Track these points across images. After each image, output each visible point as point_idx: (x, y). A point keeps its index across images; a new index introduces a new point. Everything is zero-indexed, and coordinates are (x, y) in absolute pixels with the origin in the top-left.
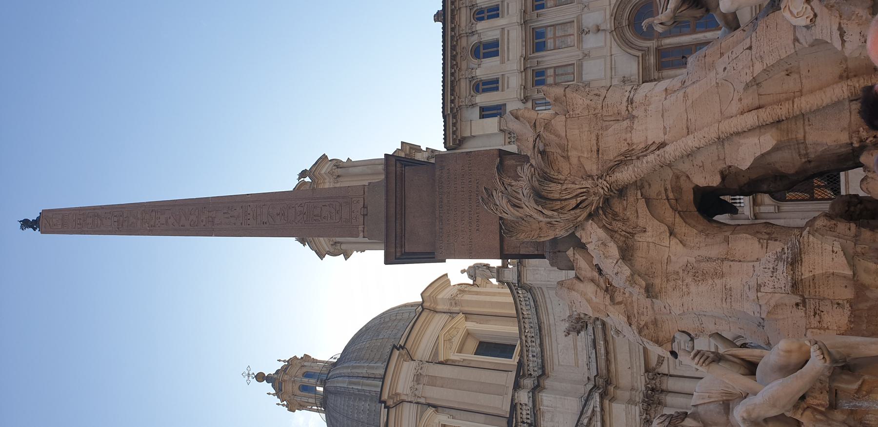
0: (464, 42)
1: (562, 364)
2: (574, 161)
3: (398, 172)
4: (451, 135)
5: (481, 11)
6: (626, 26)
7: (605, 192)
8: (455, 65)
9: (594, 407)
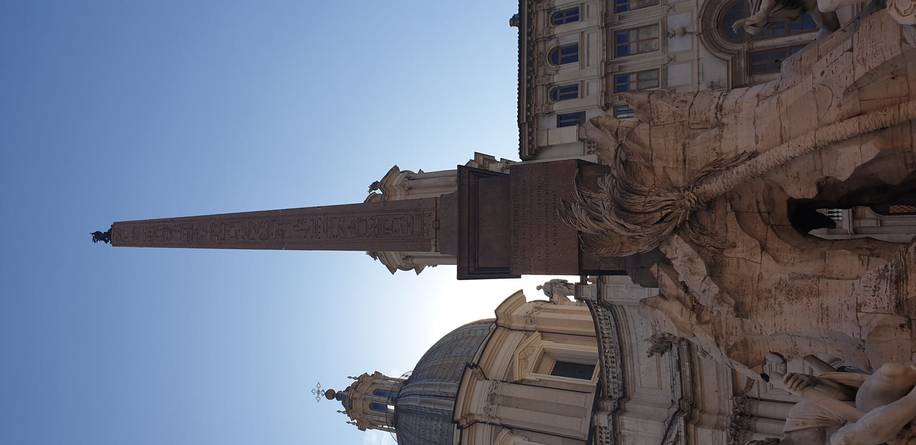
0: (541, 47)
2: (659, 171)
3: (471, 184)
4: (527, 145)
5: (559, 14)
6: (714, 28)
7: (692, 205)
8: (531, 71)
9: (678, 431)
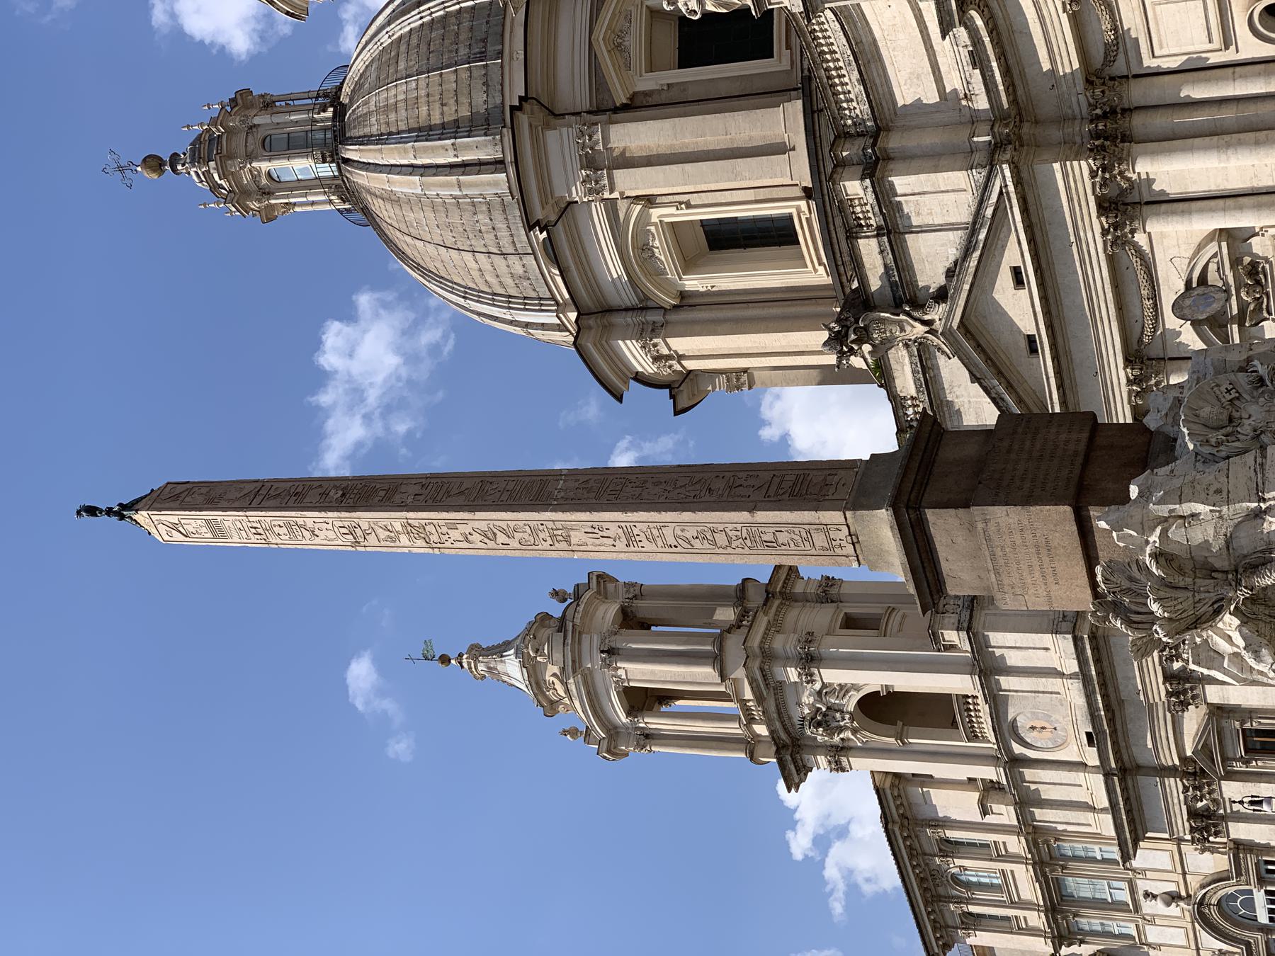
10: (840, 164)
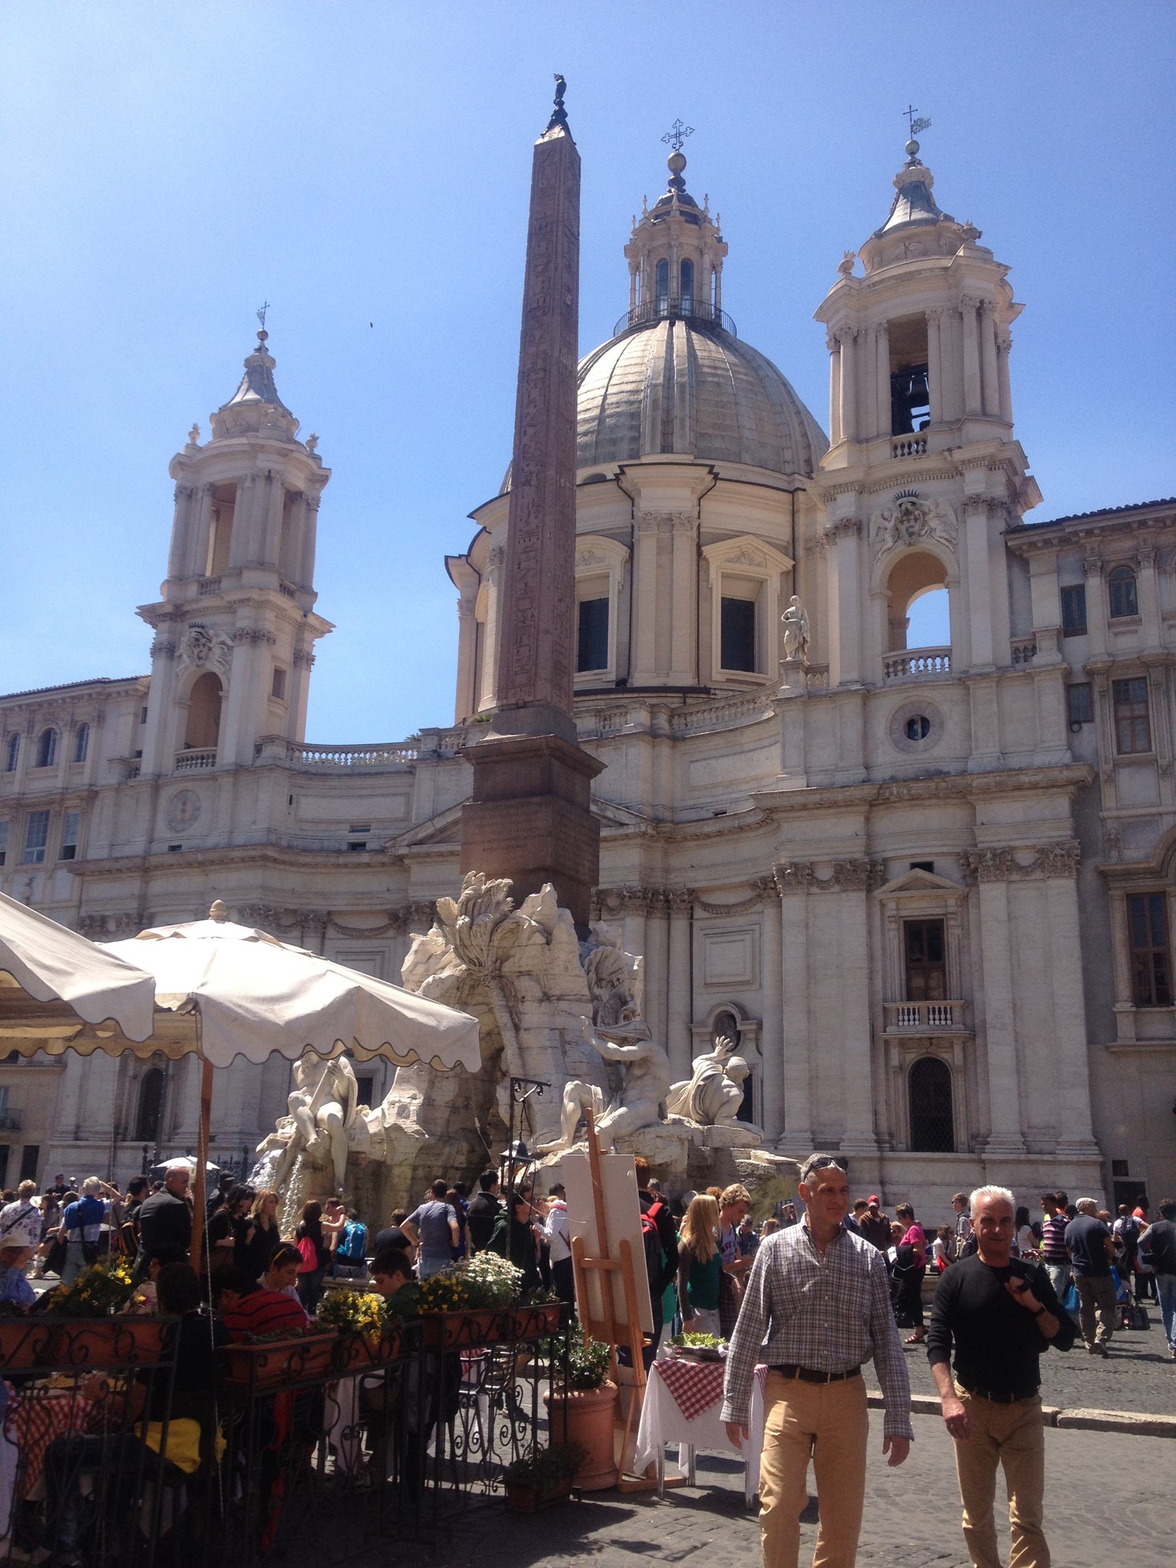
1: (692, 767)
4: (1026, 540)
10: (653, 710)
